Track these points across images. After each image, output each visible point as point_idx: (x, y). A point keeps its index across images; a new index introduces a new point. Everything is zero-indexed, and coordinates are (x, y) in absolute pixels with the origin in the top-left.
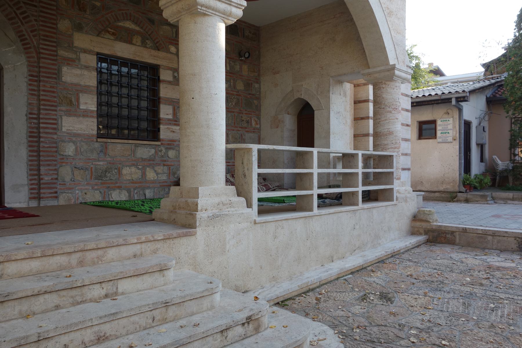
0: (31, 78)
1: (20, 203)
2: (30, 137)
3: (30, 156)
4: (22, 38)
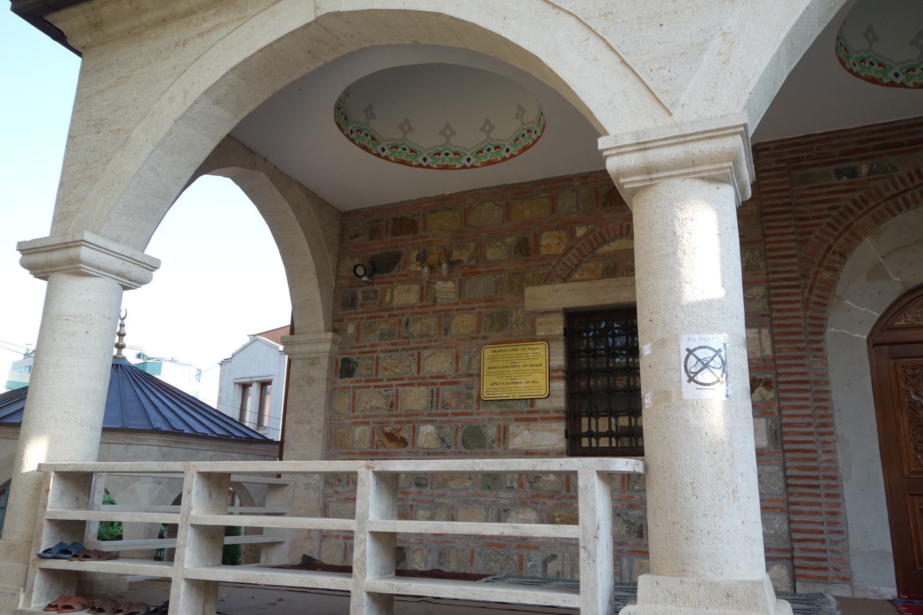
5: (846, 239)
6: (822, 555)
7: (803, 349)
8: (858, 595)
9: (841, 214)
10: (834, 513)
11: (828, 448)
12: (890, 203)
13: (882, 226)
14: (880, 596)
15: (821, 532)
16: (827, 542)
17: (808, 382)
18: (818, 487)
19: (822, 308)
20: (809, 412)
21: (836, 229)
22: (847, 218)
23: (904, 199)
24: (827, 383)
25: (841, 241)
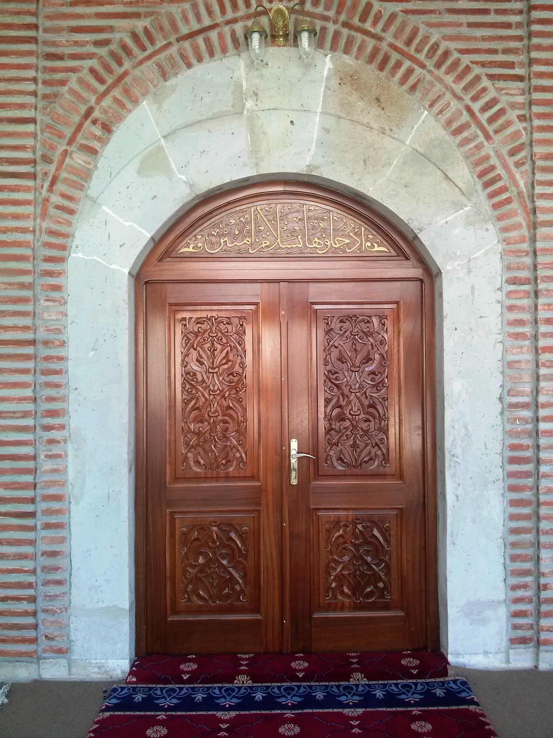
0: (512, 287)
1: (486, 653)
2: (513, 460)
3: (513, 517)
4: (487, 177)
5: (117, 101)
6: (30, 620)
7: (30, 286)
8: (79, 674)
9: (113, 54)
10: (54, 554)
11: (56, 449)
12: (186, 45)
13: (168, 83)
14: (106, 672)
15: (30, 586)
16: (39, 599)
17: (33, 342)
18: (32, 515)
19: (66, 216)
20: (28, 392)
21: (102, 81)
22: (120, 63)
23: (207, 41)
24: (63, 344)
25: (107, 102)
